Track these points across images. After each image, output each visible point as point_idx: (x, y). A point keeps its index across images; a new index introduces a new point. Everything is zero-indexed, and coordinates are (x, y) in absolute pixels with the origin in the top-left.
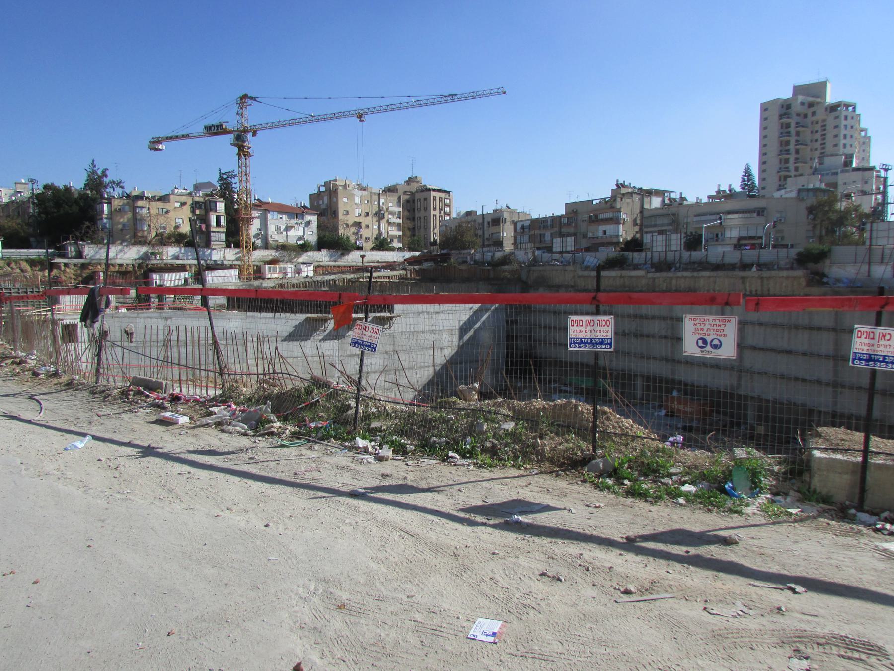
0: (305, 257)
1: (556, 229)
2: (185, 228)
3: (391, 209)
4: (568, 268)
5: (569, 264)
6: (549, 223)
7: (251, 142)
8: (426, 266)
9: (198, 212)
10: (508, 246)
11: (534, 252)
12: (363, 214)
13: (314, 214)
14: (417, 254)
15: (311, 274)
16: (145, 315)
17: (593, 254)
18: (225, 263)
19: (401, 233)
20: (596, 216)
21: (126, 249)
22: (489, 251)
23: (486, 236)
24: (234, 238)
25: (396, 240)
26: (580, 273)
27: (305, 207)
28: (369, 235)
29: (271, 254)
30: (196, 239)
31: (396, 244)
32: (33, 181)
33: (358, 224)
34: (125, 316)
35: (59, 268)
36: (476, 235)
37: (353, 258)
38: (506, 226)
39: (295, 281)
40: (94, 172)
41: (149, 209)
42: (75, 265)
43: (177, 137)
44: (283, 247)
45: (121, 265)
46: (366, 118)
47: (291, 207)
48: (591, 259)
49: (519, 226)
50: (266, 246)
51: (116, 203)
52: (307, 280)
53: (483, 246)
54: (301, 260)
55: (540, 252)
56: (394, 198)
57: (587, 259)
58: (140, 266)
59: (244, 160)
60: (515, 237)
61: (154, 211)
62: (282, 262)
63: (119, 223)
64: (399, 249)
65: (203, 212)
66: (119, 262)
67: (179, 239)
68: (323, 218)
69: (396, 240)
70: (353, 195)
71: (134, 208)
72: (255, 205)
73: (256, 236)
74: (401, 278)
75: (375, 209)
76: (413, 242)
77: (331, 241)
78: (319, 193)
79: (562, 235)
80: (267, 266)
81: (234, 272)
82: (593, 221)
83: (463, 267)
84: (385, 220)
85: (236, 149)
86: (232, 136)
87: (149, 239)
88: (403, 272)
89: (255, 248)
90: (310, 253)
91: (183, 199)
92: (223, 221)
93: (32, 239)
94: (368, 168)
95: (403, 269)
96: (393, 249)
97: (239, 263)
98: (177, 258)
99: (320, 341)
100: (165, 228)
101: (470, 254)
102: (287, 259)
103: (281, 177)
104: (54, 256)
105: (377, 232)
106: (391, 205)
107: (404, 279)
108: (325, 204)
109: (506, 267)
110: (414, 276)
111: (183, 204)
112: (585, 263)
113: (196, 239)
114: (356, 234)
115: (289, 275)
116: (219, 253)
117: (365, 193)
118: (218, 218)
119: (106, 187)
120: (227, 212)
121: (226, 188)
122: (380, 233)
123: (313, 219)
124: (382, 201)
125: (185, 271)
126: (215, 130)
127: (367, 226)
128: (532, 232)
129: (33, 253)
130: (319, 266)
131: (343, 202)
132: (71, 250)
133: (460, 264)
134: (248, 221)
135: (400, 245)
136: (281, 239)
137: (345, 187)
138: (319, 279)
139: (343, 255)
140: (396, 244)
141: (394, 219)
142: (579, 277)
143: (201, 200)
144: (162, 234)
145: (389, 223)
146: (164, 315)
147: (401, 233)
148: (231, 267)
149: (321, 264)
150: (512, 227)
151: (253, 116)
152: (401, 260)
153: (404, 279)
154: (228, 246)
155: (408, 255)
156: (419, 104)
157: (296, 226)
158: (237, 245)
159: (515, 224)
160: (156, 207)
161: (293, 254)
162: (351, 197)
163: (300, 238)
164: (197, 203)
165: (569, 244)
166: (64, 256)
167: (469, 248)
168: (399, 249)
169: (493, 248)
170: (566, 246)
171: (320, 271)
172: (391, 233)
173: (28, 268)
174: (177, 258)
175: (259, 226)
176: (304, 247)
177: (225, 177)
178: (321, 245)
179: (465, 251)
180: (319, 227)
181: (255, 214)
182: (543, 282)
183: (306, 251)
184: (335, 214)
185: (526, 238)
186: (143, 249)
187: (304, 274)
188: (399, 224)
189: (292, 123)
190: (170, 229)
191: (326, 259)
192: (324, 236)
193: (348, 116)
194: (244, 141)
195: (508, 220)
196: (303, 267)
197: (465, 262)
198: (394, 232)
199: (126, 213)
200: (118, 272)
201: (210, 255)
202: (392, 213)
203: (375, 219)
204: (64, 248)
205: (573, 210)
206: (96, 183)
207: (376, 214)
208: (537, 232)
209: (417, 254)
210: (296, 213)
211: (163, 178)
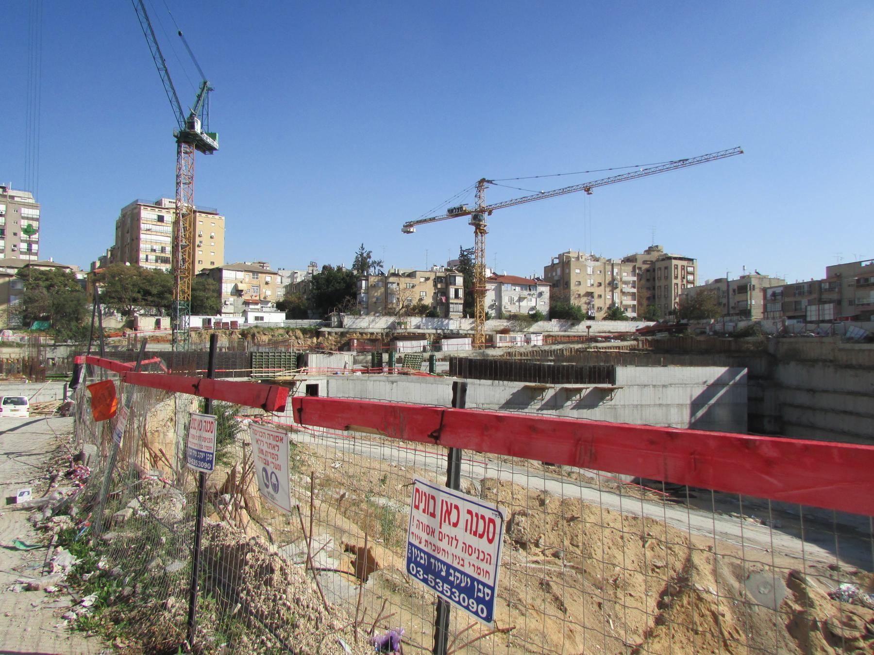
0: (535, 327)
1: (815, 296)
2: (428, 301)
3: (624, 279)
4: (824, 340)
5: (827, 335)
6: (806, 289)
7: (487, 220)
8: (659, 336)
9: (439, 286)
10: (757, 314)
11: (783, 322)
12: (596, 284)
13: (546, 285)
14: (652, 324)
15: (540, 343)
16: (375, 378)
17: (859, 324)
18: (461, 332)
19: (635, 303)
20: (867, 280)
21: (377, 320)
22: (731, 321)
23: (732, 304)
24: (470, 308)
25: (629, 310)
26: (842, 346)
27: (538, 279)
28: (602, 305)
29: (504, 324)
30: (438, 310)
31: (630, 314)
32: (313, 265)
33: (590, 294)
34: (358, 379)
35: (324, 336)
36: (720, 304)
37: (581, 329)
38: (754, 293)
39: (522, 350)
40: (362, 255)
41: (398, 284)
42: (336, 333)
43: (425, 221)
44: (513, 317)
45: (372, 334)
46: (594, 190)
47: (525, 280)
48: (856, 330)
49: (769, 292)
50: (500, 316)
51: (372, 280)
52: (535, 349)
53: (728, 314)
54: (532, 330)
55: (794, 321)
56: (629, 267)
57: (851, 328)
58: (387, 334)
59: (480, 237)
60: (765, 306)
61: (402, 286)
62: (513, 331)
63: (374, 297)
64: (633, 319)
65: (444, 286)
66: (371, 331)
67: (421, 310)
68: (556, 289)
69: (629, 310)
70: (585, 266)
71: (386, 284)
72: (490, 278)
73: (491, 307)
74: (632, 349)
75: (609, 278)
76: (649, 312)
77: (562, 311)
78: (553, 265)
79: (821, 302)
80: (498, 335)
81: (468, 341)
82: (862, 286)
83: (701, 338)
84: (618, 290)
85: (473, 228)
86: (470, 216)
87: (397, 309)
88: (635, 343)
89: (488, 317)
90: (541, 323)
91: (427, 275)
92: (461, 293)
93: (309, 312)
94: (603, 240)
95: (634, 340)
96: (626, 319)
97: (473, 332)
98: (418, 327)
99: (538, 410)
100: (411, 301)
101: (709, 324)
102: (518, 328)
103: (516, 251)
104: (321, 325)
105: (610, 302)
106: (625, 274)
107: (635, 349)
108: (558, 276)
109: (750, 339)
110: (646, 347)
111: (427, 279)
112: (848, 335)
113: (438, 310)
114: (589, 304)
115: (519, 344)
116: (457, 322)
117: (597, 263)
118: (457, 291)
119: (369, 267)
120: (465, 283)
121: (465, 264)
122: (613, 303)
123: (546, 290)
124: (616, 270)
125: (425, 339)
126: (456, 212)
127: (600, 296)
128: (787, 299)
129: (306, 323)
130: (549, 336)
131: (575, 273)
132: (335, 320)
133: (697, 335)
134: (483, 293)
135: (635, 315)
136: (514, 309)
137: (578, 258)
138: (547, 348)
139: (573, 325)
140: (630, 314)
141: (628, 289)
142: (840, 350)
143: (442, 275)
144: (407, 306)
145: (623, 293)
146: (391, 379)
147: (635, 303)
148: (465, 336)
149: (551, 334)
150: (761, 294)
151: (489, 197)
152: (634, 330)
153: (635, 349)
154: (465, 317)
155: (642, 324)
156: (647, 173)
157: (529, 297)
158: (472, 316)
159: (764, 290)
160: (404, 281)
161: (524, 324)
162: (583, 268)
163: (533, 308)
164: (439, 277)
165: (827, 312)
166: (328, 325)
167: (708, 317)
168: (633, 319)
169: (735, 318)
170: (823, 315)
171: (550, 340)
172: (624, 303)
173: (301, 336)
174: (418, 327)
175: (494, 298)
176: (535, 317)
177: (465, 253)
178: (553, 314)
179: (705, 321)
180: (552, 297)
181: (490, 287)
182: (795, 356)
183: (537, 321)
184: (567, 284)
185: (778, 306)
186: (391, 320)
187: (532, 344)
188: (633, 294)
189: (524, 200)
190: (415, 302)
191: (557, 329)
192: (556, 307)
193: (576, 190)
194: (480, 220)
195: (757, 286)
196: (533, 337)
197: (703, 333)
198: (628, 301)
199: (379, 288)
200: (369, 340)
201: (448, 324)
202: (626, 283)
203: (608, 289)
204: (329, 319)
205: (836, 274)
206: (362, 263)
207: (609, 284)
208: (792, 299)
209: (652, 324)
210: (529, 285)
211: (414, 259)
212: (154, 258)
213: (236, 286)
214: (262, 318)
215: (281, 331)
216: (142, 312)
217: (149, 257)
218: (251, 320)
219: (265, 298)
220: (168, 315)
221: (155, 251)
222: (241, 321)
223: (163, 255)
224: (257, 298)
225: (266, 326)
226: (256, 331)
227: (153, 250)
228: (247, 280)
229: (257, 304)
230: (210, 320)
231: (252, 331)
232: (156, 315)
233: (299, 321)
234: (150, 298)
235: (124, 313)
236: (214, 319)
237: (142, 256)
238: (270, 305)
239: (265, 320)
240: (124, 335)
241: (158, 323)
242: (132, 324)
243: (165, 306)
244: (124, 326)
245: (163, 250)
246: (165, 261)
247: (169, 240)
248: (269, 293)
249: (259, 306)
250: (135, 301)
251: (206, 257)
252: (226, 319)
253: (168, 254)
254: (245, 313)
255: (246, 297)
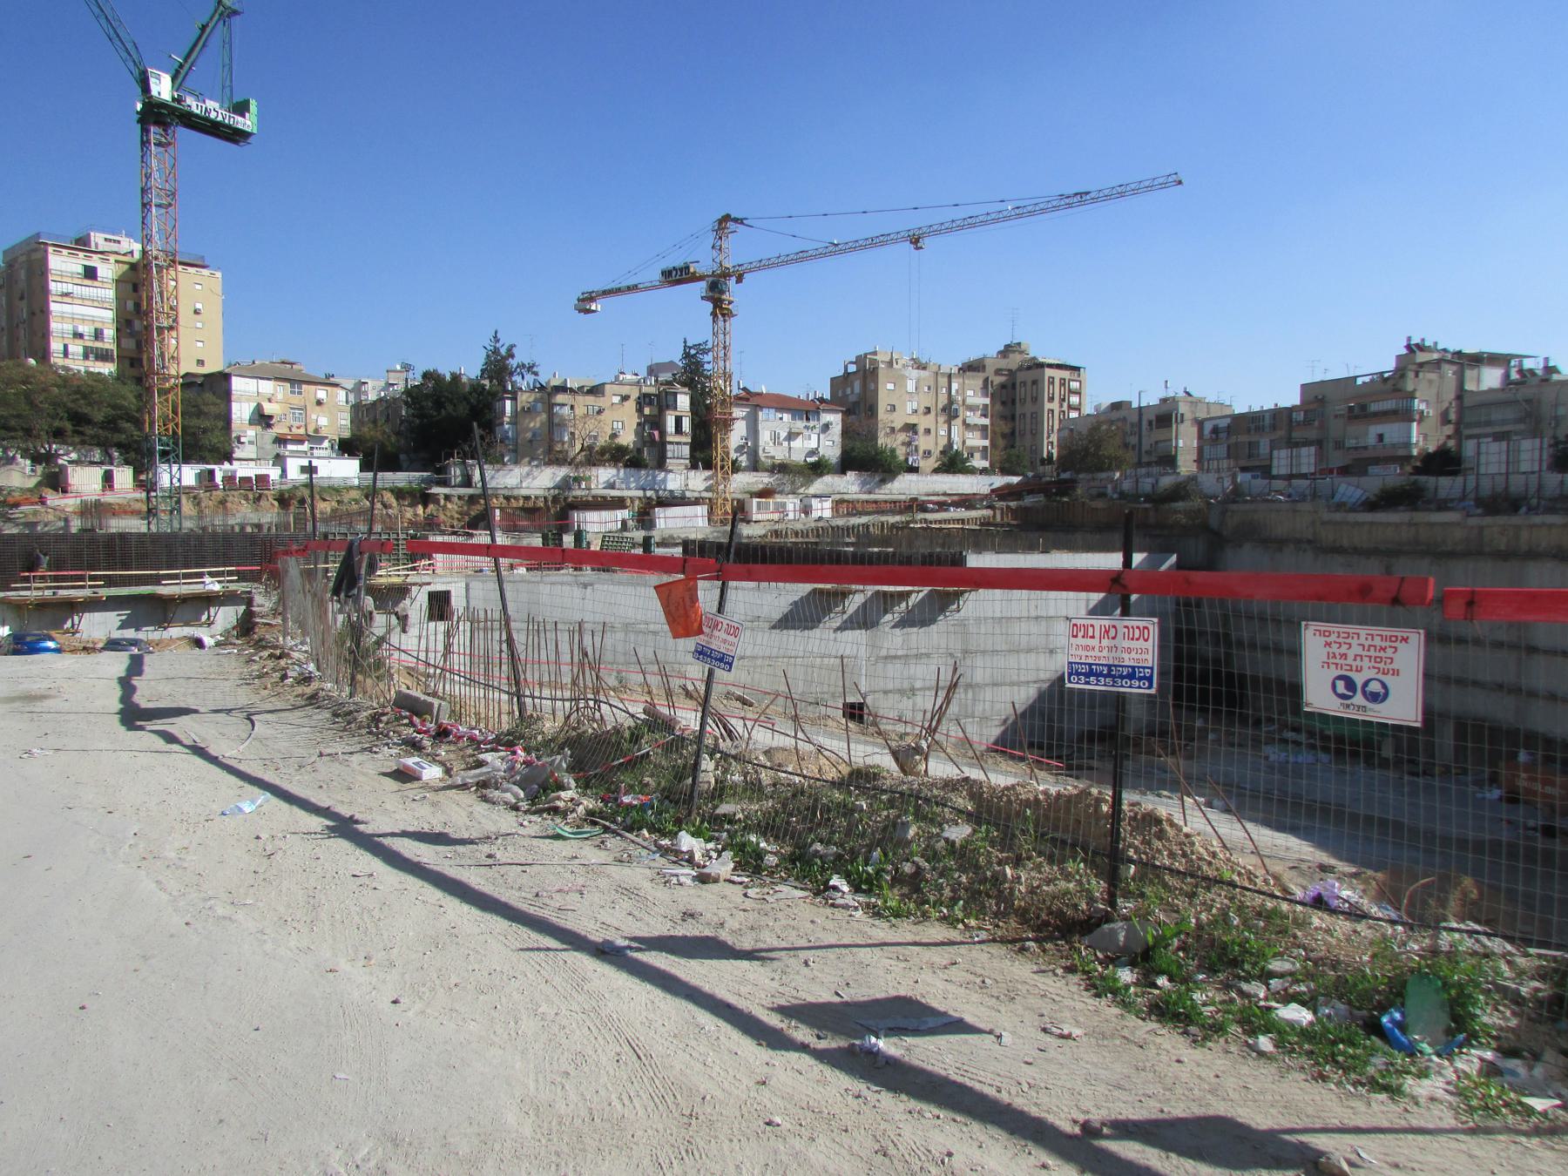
0: (819, 485)
1: (1281, 433)
2: (628, 438)
3: (969, 401)
4: (1299, 506)
5: (1303, 498)
6: (1267, 421)
7: (734, 292)
8: (1029, 501)
9: (647, 411)
10: (1186, 465)
11: (1234, 477)
12: (921, 410)
13: (835, 411)
14: (1015, 480)
15: (827, 514)
16: (553, 579)
17: (1354, 480)
18: (688, 494)
19: (987, 443)
20: (1363, 407)
21: (536, 472)
22: (1148, 475)
23: (1145, 447)
24: (703, 453)
25: (977, 455)
26: (1326, 516)
27: (822, 400)
28: (930, 447)
29: (763, 480)
30: (645, 455)
31: (978, 462)
32: (407, 368)
33: (911, 428)
34: (523, 581)
35: (437, 502)
36: (1126, 446)
37: (903, 486)
38: (1182, 427)
39: (799, 526)
40: (496, 351)
41: (572, 407)
42: (460, 498)
43: (617, 291)
44: (782, 468)
45: (527, 498)
46: (926, 243)
47: (798, 400)
48: (1349, 490)
49: (1208, 427)
50: (755, 466)
51: (525, 399)
52: (820, 524)
53: (1140, 464)
54: (812, 490)
55: (1248, 476)
56: (976, 381)
57: (1343, 487)
58: (555, 499)
59: (721, 323)
60: (1200, 450)
61: (580, 411)
62: (781, 492)
63: (528, 429)
64: (984, 471)
65: (656, 412)
66: (524, 492)
67: (615, 455)
68: (852, 418)
69: (977, 455)
70: (904, 378)
71: (551, 406)
72: (738, 398)
73: (740, 449)
74: (985, 523)
75: (943, 400)
76: (1008, 460)
77: (863, 457)
78: (847, 375)
79: (1292, 444)
80: (755, 500)
81: (701, 510)
82: (1356, 417)
83: (1099, 504)
84: (959, 421)
85: (709, 306)
86: (703, 285)
87: (571, 454)
88: (988, 512)
89: (736, 468)
90: (828, 479)
91: (625, 390)
92: (686, 425)
93: (402, 457)
94: (931, 331)
95: (989, 507)
96: (972, 471)
97: (709, 495)
98: (612, 486)
99: (838, 629)
100: (595, 437)
101: (1112, 480)
102: (788, 488)
103: (782, 351)
104: (430, 482)
105: (944, 441)
106: (970, 393)
107: (989, 524)
108: (855, 395)
109: (1180, 505)
110: (1008, 519)
111: (625, 398)
112: (1337, 498)
113: (645, 455)
114: (909, 444)
115: (791, 516)
116: (680, 478)
117: (923, 373)
118: (678, 421)
119: (511, 374)
120: (694, 409)
121: (692, 372)
122: (950, 444)
123: (835, 419)
124: (955, 386)
125: (625, 507)
126: (677, 276)
127: (928, 431)
128: (1233, 439)
129: (401, 478)
130: (842, 501)
131: (886, 390)
132: (456, 473)
133: (1092, 498)
134: (727, 424)
135: (986, 464)
136: (779, 454)
137: (890, 364)
138: (840, 522)
139: (883, 481)
140: (978, 462)
141: (976, 419)
142: (1323, 523)
143: (653, 390)
144: (590, 448)
145: (967, 426)
146: (582, 579)
147: (987, 443)
148: (697, 502)
149: (846, 497)
150: (1195, 430)
151: (738, 249)
152: (986, 490)
153: (989, 524)
154: (694, 467)
155: (999, 481)
156: (1020, 213)
157: (806, 433)
158: (708, 465)
159: (1200, 424)
160: (583, 402)
161: (799, 480)
162: (899, 380)
163: (812, 453)
164: (645, 395)
165: (1304, 460)
166: (444, 483)
167: (1109, 469)
168: (984, 471)
169: (1155, 470)
170: (1299, 465)
171: (843, 509)
172: (969, 443)
173: (394, 502)
174: (612, 486)
175: (744, 433)
176: (818, 468)
177: (693, 352)
178: (847, 463)
179: (1104, 475)
180: (845, 433)
181: (738, 412)
182: (1252, 534)
183: (821, 475)
184: (872, 410)
185: (1222, 450)
186: (562, 472)
187: (815, 514)
188: (984, 428)
189: (802, 257)
190: (602, 441)
191: (855, 488)
192: (853, 449)
193: (895, 241)
194: (722, 292)
195: (1188, 416)
196: (815, 503)
197: (1102, 495)
198: (976, 441)
199: (539, 413)
200: (523, 509)
201: (664, 481)
202: (972, 408)
203: (941, 419)
204: (442, 470)
205: (1317, 397)
206: (498, 367)
207: (944, 410)
208: (1243, 438)
209: (1015, 480)
210: (806, 410)
211: (598, 360)
212: (81, 350)
213: (259, 407)
215: (355, 494)
216: (74, 456)
217: (71, 349)
219: (316, 431)
220: (127, 463)
221: (81, 336)
222: (274, 473)
223: (98, 345)
224: (302, 431)
225: (325, 484)
227: (78, 336)
228: (280, 396)
229: (301, 442)
230: (212, 472)
231: (299, 494)
232: (101, 463)
234: (89, 431)
235: (36, 459)
236: (220, 471)
237: (56, 346)
238: (326, 444)
240: (42, 501)
241: (108, 479)
242: (56, 481)
243: (119, 446)
244: (39, 484)
245: (98, 335)
246: (103, 356)
248: (323, 421)
249: (305, 447)
250: (58, 435)
252: (243, 470)
253: (109, 342)
254: (279, 460)
255: (279, 429)
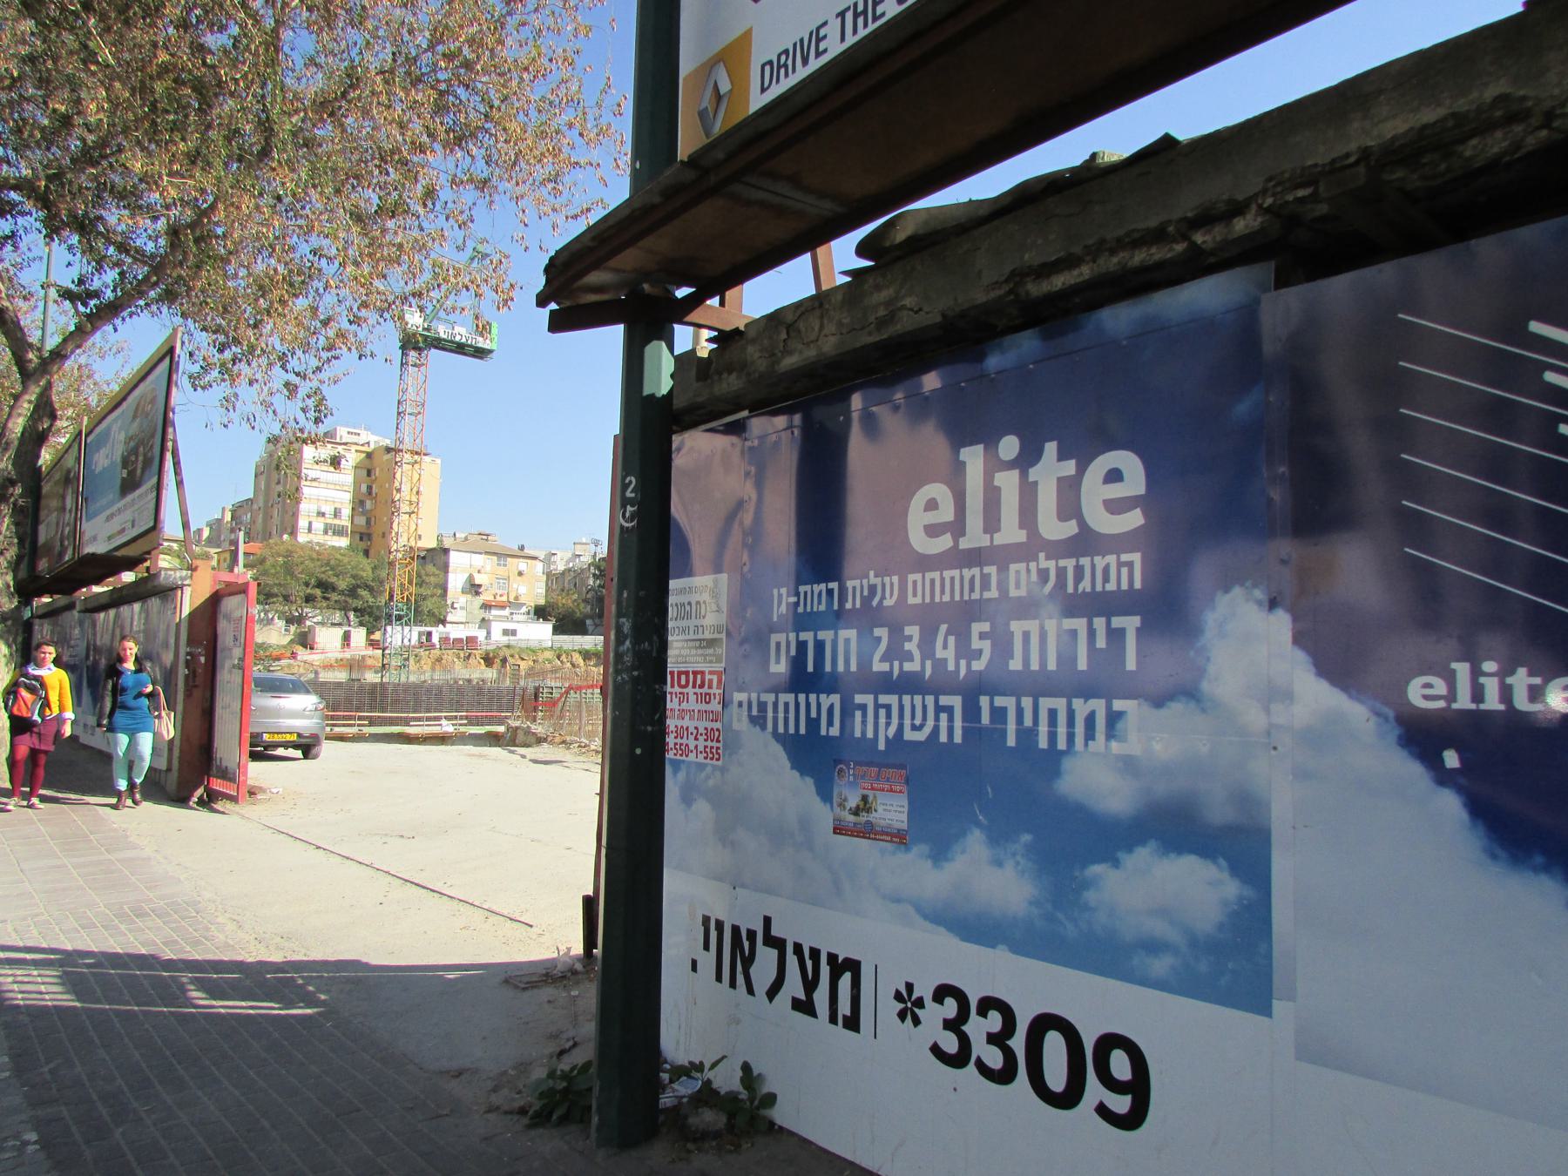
93: (588, 622)
212: (322, 527)
213: (471, 577)
214: (514, 633)
215: (548, 655)
216: (319, 618)
217: (314, 526)
218: (497, 636)
219: (517, 598)
220: (361, 624)
221: (323, 515)
222: (481, 635)
223: (337, 522)
224: (505, 599)
225: (523, 645)
226: (507, 653)
227: (321, 514)
228: (488, 568)
229: (503, 607)
230: (429, 634)
231: (502, 654)
232: (340, 624)
233: (578, 638)
234: (334, 597)
235: (290, 621)
236: (437, 632)
237: (303, 523)
238: (524, 609)
239: (519, 636)
240: (294, 655)
241: (347, 637)
242: (305, 640)
243: (355, 610)
244: (292, 641)
245: (337, 513)
246: (339, 532)
247: (348, 497)
248: (523, 590)
249: (506, 612)
250: (309, 599)
251: (417, 528)
252: (456, 632)
253: (345, 521)
254: (484, 623)
255: (486, 596)
